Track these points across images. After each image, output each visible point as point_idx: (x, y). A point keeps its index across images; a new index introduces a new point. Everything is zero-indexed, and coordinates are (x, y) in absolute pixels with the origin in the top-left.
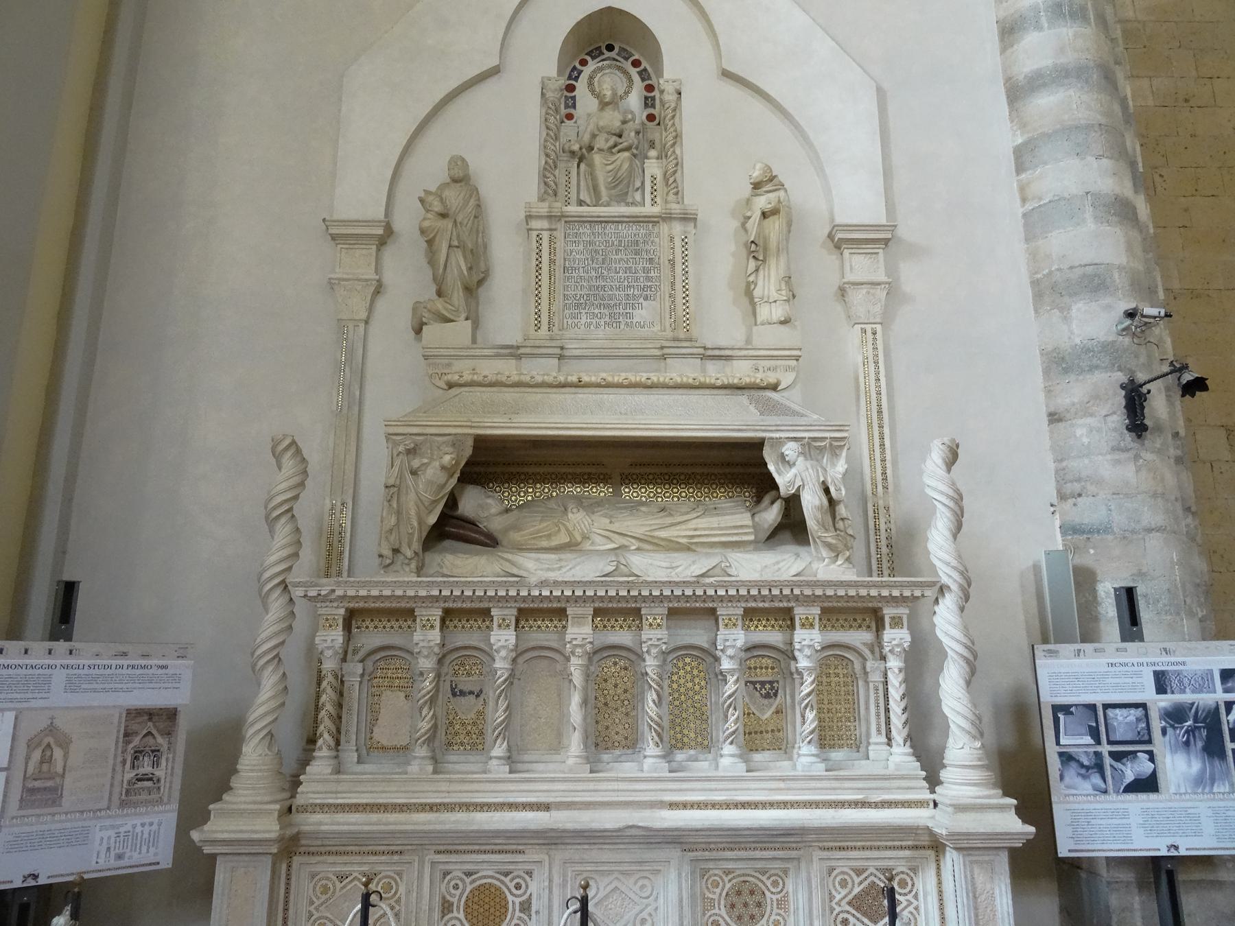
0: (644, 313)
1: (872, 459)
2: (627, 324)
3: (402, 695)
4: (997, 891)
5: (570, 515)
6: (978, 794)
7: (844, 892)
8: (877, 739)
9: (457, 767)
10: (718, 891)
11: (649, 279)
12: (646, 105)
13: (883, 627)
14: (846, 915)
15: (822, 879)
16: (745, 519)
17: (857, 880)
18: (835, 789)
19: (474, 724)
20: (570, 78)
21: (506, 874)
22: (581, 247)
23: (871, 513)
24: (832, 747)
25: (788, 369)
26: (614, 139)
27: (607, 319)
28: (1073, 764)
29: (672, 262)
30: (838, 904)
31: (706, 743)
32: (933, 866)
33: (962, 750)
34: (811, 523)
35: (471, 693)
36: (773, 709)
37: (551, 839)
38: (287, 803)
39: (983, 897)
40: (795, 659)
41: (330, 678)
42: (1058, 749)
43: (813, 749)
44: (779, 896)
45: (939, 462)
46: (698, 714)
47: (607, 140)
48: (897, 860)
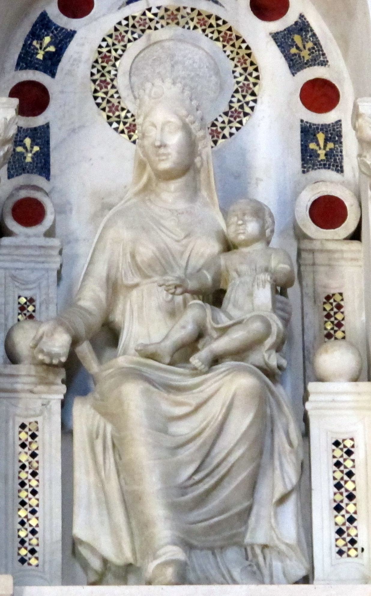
12: (308, 159)
20: (26, 60)
26: (195, 312)
47: (173, 313)
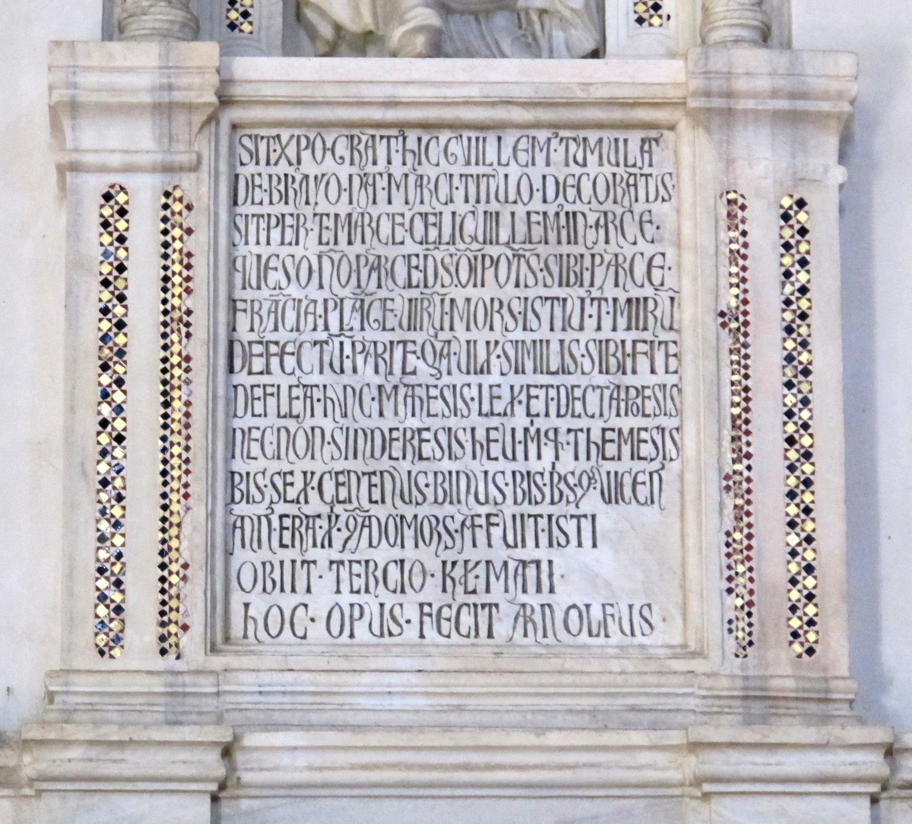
0: (594, 568)
2: (523, 616)
11: (626, 400)
22: (309, 247)
27: (432, 593)
29: (735, 322)
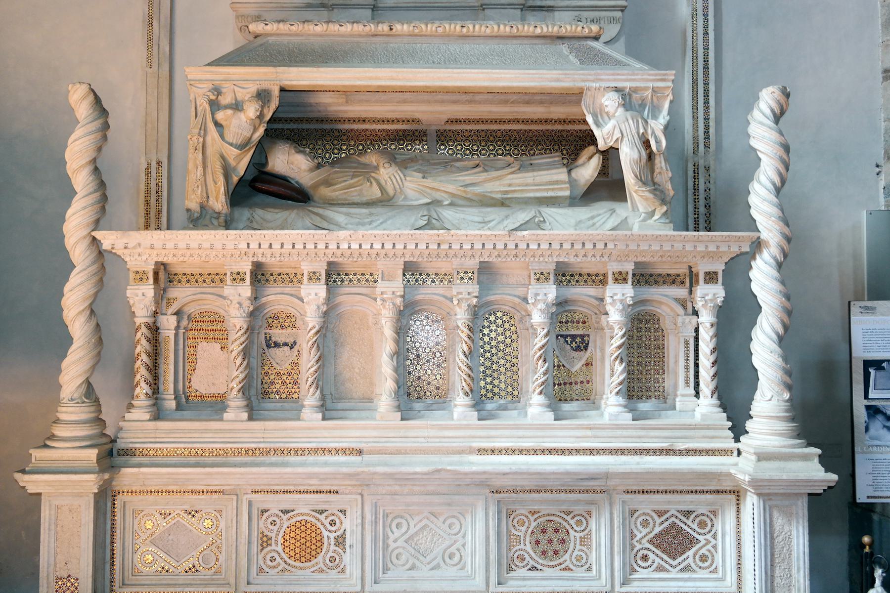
1: (695, 117)
3: (218, 346)
4: (794, 533)
5: (382, 170)
6: (782, 443)
7: (645, 531)
8: (685, 391)
9: (272, 413)
10: (524, 529)
13: (697, 282)
14: (646, 552)
15: (624, 519)
16: (561, 174)
17: (658, 521)
18: (640, 437)
19: (289, 374)
21: (321, 512)
23: (690, 173)
24: (640, 398)
25: (612, 20)
28: (880, 417)
30: (639, 542)
31: (516, 393)
32: (733, 509)
33: (769, 401)
34: (629, 179)
35: (285, 344)
36: (583, 362)
37: (363, 483)
38: (109, 446)
39: (780, 539)
40: (607, 314)
41: (144, 329)
42: (866, 402)
43: (621, 400)
44: (582, 534)
45: (768, 112)
46: (508, 365)
48: (700, 504)
